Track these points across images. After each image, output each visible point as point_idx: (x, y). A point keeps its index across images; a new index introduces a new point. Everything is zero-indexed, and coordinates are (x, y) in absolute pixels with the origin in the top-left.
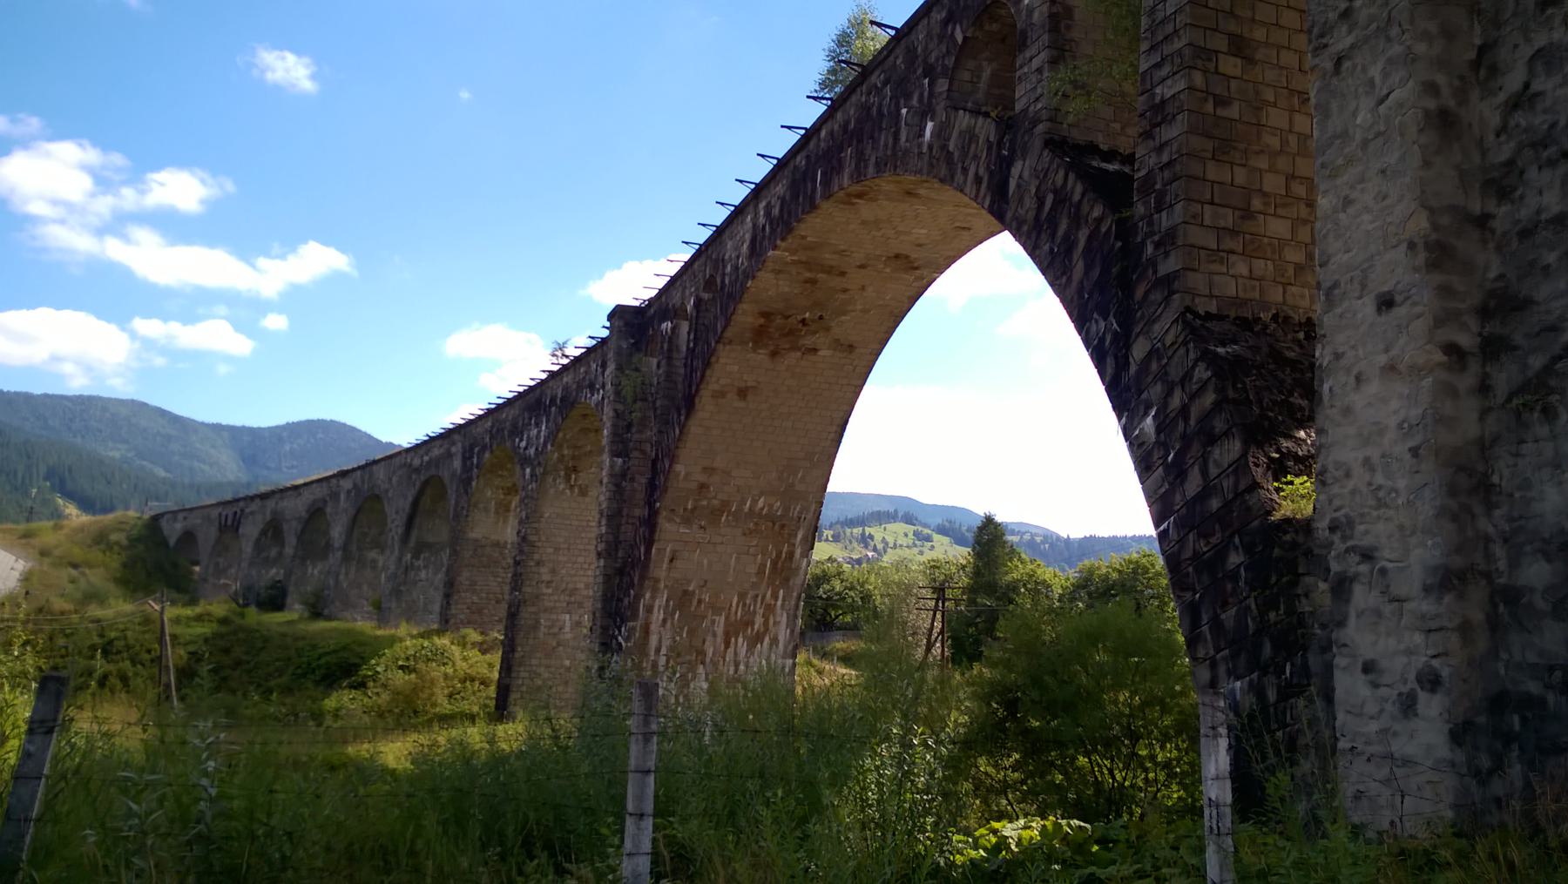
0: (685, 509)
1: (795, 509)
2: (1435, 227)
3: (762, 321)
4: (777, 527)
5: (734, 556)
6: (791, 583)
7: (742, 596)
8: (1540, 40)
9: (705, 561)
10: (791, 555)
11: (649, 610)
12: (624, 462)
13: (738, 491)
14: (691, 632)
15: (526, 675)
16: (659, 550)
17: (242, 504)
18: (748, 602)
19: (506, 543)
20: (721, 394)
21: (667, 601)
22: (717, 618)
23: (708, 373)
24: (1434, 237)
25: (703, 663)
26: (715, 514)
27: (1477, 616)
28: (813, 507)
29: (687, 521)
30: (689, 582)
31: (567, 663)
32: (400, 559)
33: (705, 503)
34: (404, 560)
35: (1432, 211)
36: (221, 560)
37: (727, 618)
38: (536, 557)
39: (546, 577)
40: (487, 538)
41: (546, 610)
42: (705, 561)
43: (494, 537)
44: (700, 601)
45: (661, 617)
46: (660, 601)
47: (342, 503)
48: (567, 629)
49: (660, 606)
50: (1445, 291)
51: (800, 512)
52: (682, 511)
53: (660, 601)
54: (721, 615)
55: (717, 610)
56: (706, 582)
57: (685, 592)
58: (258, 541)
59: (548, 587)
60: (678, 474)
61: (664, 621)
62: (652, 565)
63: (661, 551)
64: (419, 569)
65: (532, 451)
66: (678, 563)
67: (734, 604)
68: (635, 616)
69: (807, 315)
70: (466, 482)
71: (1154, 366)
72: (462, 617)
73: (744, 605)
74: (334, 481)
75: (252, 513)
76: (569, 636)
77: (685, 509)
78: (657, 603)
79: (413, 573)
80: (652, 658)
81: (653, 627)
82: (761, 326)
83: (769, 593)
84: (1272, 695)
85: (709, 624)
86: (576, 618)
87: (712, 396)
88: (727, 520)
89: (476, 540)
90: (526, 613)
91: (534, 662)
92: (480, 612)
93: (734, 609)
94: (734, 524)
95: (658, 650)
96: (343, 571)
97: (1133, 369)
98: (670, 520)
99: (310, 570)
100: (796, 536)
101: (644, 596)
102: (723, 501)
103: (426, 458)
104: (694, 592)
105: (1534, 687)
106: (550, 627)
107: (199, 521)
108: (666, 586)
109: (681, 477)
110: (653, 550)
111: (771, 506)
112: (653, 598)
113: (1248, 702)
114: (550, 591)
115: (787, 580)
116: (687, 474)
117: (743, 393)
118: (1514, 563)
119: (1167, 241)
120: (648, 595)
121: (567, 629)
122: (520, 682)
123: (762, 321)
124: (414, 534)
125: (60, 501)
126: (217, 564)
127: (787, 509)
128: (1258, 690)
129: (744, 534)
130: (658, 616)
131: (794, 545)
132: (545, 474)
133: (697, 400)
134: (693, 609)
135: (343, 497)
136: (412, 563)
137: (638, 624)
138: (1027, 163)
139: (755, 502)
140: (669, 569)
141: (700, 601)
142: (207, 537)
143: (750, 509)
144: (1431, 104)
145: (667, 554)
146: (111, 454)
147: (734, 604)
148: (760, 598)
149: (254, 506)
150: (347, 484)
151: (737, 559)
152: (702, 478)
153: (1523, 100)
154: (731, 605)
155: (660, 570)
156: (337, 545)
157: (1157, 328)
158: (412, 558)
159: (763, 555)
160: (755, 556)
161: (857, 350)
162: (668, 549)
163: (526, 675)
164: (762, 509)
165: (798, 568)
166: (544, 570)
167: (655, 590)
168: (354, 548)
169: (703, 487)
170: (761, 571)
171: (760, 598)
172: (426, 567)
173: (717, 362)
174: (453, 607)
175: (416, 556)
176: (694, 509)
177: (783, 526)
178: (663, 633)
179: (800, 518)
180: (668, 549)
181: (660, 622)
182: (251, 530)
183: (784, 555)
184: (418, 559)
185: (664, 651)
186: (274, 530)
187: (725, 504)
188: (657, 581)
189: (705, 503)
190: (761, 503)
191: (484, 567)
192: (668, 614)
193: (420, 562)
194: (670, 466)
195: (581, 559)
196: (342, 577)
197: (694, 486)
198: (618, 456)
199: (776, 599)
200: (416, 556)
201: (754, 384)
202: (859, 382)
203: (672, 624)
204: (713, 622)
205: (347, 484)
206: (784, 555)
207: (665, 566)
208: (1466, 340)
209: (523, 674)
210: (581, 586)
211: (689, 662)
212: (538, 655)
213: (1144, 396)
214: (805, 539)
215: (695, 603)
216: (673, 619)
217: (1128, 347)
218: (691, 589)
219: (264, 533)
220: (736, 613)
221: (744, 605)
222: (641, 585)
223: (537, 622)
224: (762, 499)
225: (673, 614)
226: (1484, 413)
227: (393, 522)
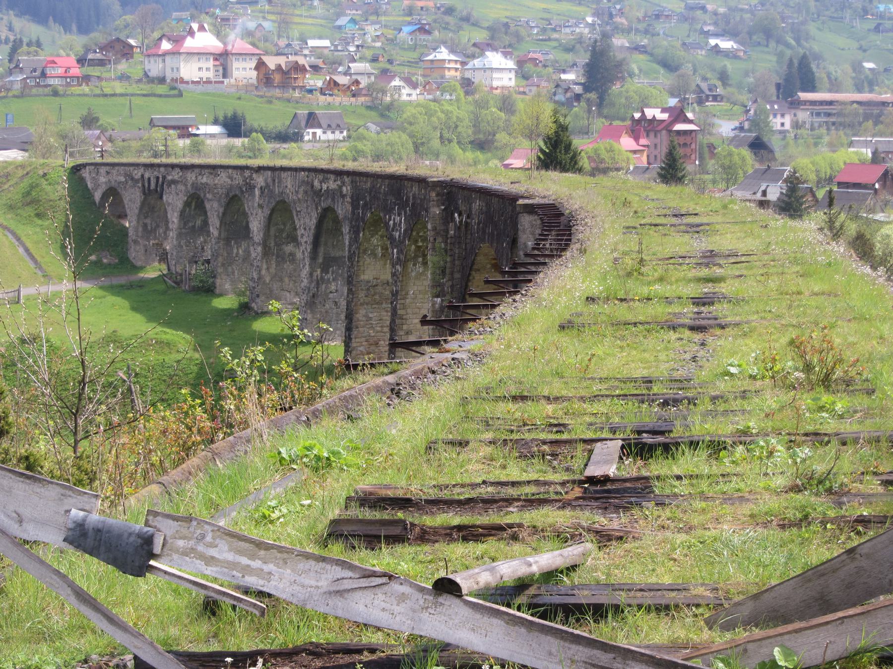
12: (442, 300)
17: (162, 169)
32: (311, 275)
34: (315, 274)
36: (148, 221)
38: (405, 327)
40: (377, 279)
58: (182, 214)
64: (328, 281)
72: (361, 348)
75: (174, 182)
79: (324, 286)
89: (368, 282)
96: (265, 266)
99: (235, 251)
107: (122, 179)
124: (321, 250)
126: (145, 225)
135: (257, 192)
136: (322, 278)
142: (132, 199)
149: (175, 175)
150: (260, 180)
158: (322, 272)
174: (353, 340)
175: (325, 269)
184: (327, 273)
191: (377, 303)
193: (329, 276)
196: (263, 272)
198: (437, 296)
219: (187, 204)
227: (302, 237)
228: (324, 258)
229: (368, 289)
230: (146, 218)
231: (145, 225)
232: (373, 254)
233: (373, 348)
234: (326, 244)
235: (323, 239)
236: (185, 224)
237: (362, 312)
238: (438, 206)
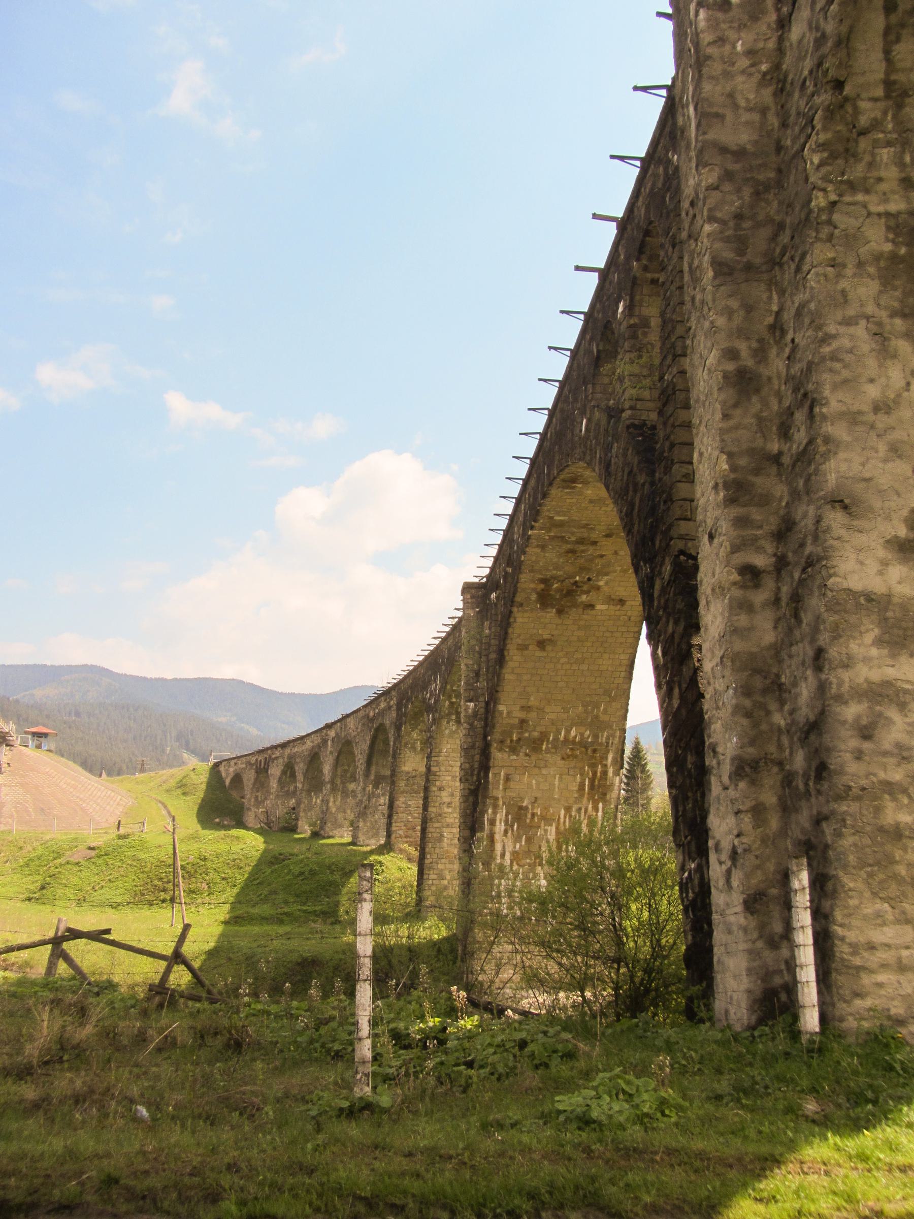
0: (512, 741)
1: (602, 736)
2: (734, 468)
3: (542, 586)
4: (589, 751)
5: (557, 777)
6: (608, 796)
7: (568, 809)
9: (534, 782)
10: (605, 773)
11: (492, 823)
12: (476, 705)
13: (553, 724)
14: (529, 840)
15: (435, 877)
16: (495, 775)
17: (269, 752)
18: (573, 814)
20: (523, 648)
21: (507, 815)
22: (549, 828)
23: (510, 630)
24: (732, 476)
25: (541, 864)
26: (536, 745)
27: (770, 798)
28: (618, 733)
29: (514, 750)
30: (522, 799)
32: (364, 789)
33: (527, 735)
34: (368, 789)
35: (730, 455)
36: (259, 794)
37: (557, 828)
38: (438, 783)
41: (448, 826)
42: (534, 782)
44: (533, 815)
45: (503, 827)
46: (501, 815)
47: (329, 748)
49: (501, 820)
50: (741, 522)
51: (608, 738)
52: (509, 742)
53: (501, 815)
54: (551, 825)
55: (548, 820)
56: (536, 798)
57: (521, 808)
58: (280, 779)
59: (448, 807)
60: (501, 713)
61: (506, 832)
62: (490, 787)
63: (497, 775)
64: (378, 796)
65: (432, 701)
66: (512, 784)
67: (562, 816)
68: (482, 829)
69: (578, 578)
70: (398, 728)
72: (401, 832)
73: (570, 816)
74: (324, 731)
75: (277, 758)
77: (512, 741)
78: (498, 816)
79: (374, 800)
80: (498, 861)
81: (498, 837)
82: (543, 590)
83: (590, 806)
85: (543, 832)
87: (517, 649)
88: (547, 748)
89: (408, 773)
90: (432, 828)
91: (440, 866)
93: (562, 820)
94: (553, 750)
95: (503, 855)
96: (332, 800)
98: (500, 750)
99: (314, 800)
100: (607, 758)
101: (486, 811)
102: (541, 733)
103: (377, 711)
104: (527, 808)
106: (451, 840)
107: (244, 766)
108: (504, 803)
109: (505, 715)
110: (490, 775)
111: (582, 735)
112: (495, 813)
114: (450, 810)
115: (605, 794)
116: (508, 713)
117: (541, 644)
120: (490, 811)
122: (430, 882)
123: (542, 586)
124: (373, 769)
125: (185, 755)
126: (257, 797)
127: (596, 737)
129: (563, 759)
130: (500, 827)
131: (606, 765)
132: (441, 718)
133: (506, 653)
134: (528, 821)
135: (329, 743)
136: (373, 792)
137: (485, 834)
139: (568, 732)
140: (505, 789)
141: (533, 815)
142: (249, 777)
143: (565, 738)
144: (730, 367)
145: (502, 777)
146: (220, 720)
147: (562, 816)
148: (583, 810)
149: (277, 753)
150: (332, 733)
151: (561, 779)
152: (522, 715)
154: (559, 817)
155: (498, 791)
156: (327, 780)
158: (373, 788)
159: (582, 775)
160: (575, 776)
161: (627, 603)
162: (502, 774)
163: (435, 877)
164: (575, 737)
165: (612, 785)
166: (444, 794)
167: (495, 807)
168: (338, 781)
169: (523, 722)
170: (582, 785)
171: (583, 810)
172: (383, 795)
173: (515, 621)
174: (394, 824)
175: (376, 786)
176: (519, 739)
177: (595, 751)
178: (506, 841)
179: (608, 743)
180: (502, 774)
181: (502, 832)
182: (275, 771)
183: (599, 775)
184: (377, 788)
185: (508, 857)
186: (289, 770)
187: (543, 737)
188: (497, 799)
189: (527, 735)
190: (573, 733)
191: (415, 793)
192: (509, 825)
193: (379, 791)
194: (495, 707)
196: (331, 804)
197: (516, 721)
198: (470, 701)
199: (597, 810)
200: (376, 786)
201: (549, 637)
202: (636, 629)
203: (512, 834)
204: (546, 831)
205: (332, 733)
206: (599, 775)
207: (501, 787)
208: (761, 561)
209: (432, 877)
211: (530, 865)
212: (443, 861)
214: (614, 759)
215: (529, 816)
216: (513, 830)
218: (524, 804)
219: (284, 772)
220: (565, 822)
221: (570, 816)
222: (484, 803)
223: (442, 836)
224: (574, 729)
225: (512, 826)
228: (376, 776)
229: (408, 780)
230: (258, 791)
231: (257, 797)
232: (414, 748)
233: (410, 832)
234: (377, 764)
235: (374, 760)
236: (282, 788)
237: (402, 799)
238: (473, 609)
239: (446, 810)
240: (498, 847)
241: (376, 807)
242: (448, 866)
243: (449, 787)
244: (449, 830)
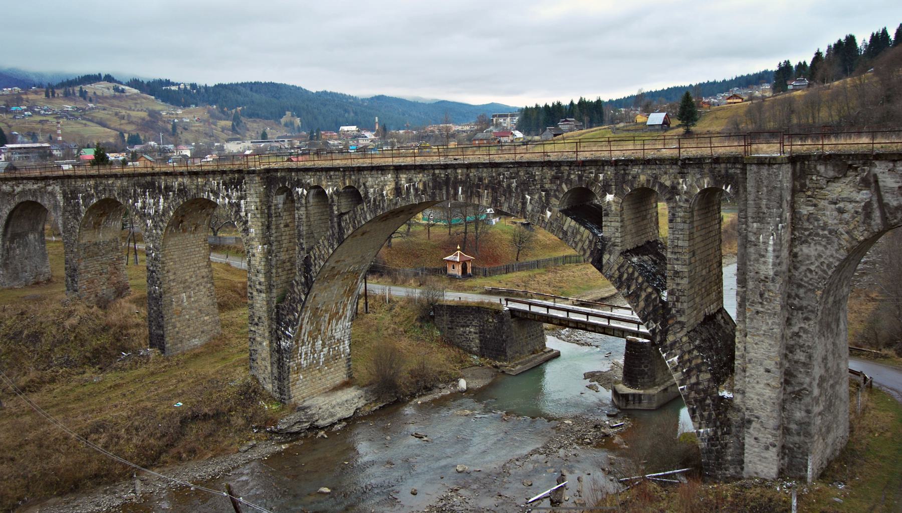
8: (803, 325)
11: (303, 320)
19: (100, 242)
31: (187, 317)
34: (6, 245)
39: (172, 278)
41: (175, 294)
43: (94, 240)
48: (185, 301)
64: (15, 249)
71: (677, 345)
76: (186, 304)
81: (304, 326)
84: (719, 433)
86: (188, 294)
91: (173, 320)
92: (93, 282)
97: (668, 342)
105: (791, 446)
106: (177, 302)
113: (712, 434)
118: (789, 423)
119: (681, 312)
121: (185, 301)
124: (10, 229)
128: (716, 433)
130: (306, 320)
137: (298, 327)
138: (612, 257)
153: (797, 334)
157: (679, 335)
158: (10, 243)
166: (170, 274)
167: (306, 311)
172: (18, 247)
193: (15, 245)
195: (186, 264)
210: (187, 277)
213: (673, 351)
217: (666, 335)
223: (172, 301)
226: (784, 394)
237: (83, 264)
239: (172, 284)
240: (303, 331)
241: (14, 257)
242: (177, 319)
243: (173, 269)
244: (175, 296)
